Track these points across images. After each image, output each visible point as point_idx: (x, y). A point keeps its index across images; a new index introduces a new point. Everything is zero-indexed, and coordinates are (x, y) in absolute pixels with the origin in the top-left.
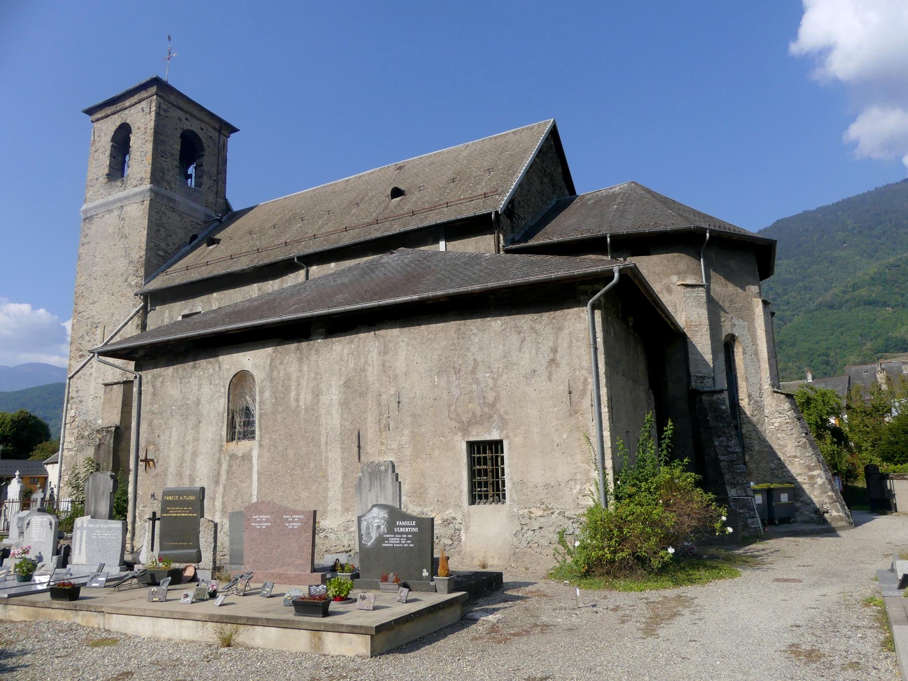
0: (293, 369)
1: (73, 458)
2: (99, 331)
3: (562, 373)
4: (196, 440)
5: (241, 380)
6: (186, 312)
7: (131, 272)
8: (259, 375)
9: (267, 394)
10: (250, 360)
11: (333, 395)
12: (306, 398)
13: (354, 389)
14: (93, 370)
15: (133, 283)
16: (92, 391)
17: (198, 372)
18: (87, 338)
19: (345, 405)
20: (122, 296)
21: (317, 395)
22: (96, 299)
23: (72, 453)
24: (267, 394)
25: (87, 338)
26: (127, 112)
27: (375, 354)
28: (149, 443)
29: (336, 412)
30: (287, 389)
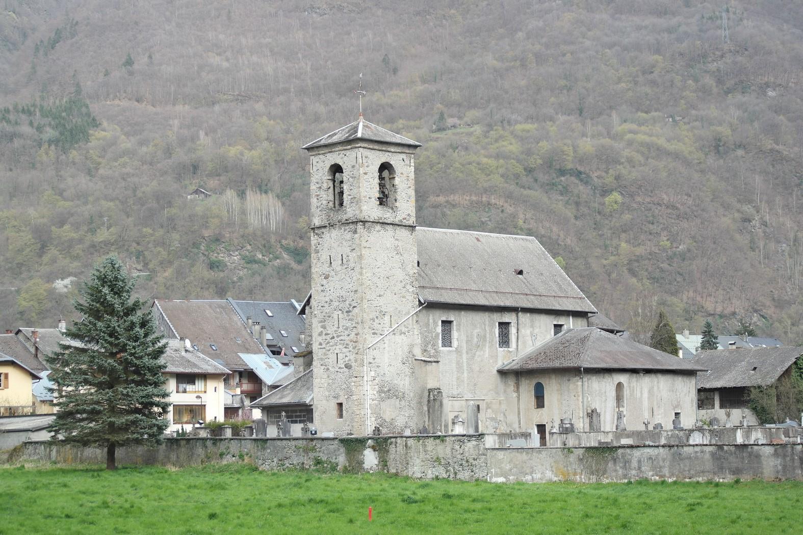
0: (635, 384)
1: (377, 406)
2: (387, 318)
3: (690, 395)
4: (605, 407)
5: (619, 386)
6: (444, 319)
7: (408, 282)
8: (625, 385)
9: (628, 392)
10: (623, 378)
11: (646, 395)
12: (639, 395)
13: (651, 392)
14: (386, 345)
15: (411, 290)
16: (387, 360)
17: (605, 380)
18: (377, 321)
19: (649, 398)
20: (404, 297)
21: (642, 393)
22: (382, 293)
23: (376, 402)
24: (628, 392)
25: (377, 321)
26: (390, 154)
27: (656, 383)
28: (587, 407)
29: (646, 399)
30: (633, 390)
